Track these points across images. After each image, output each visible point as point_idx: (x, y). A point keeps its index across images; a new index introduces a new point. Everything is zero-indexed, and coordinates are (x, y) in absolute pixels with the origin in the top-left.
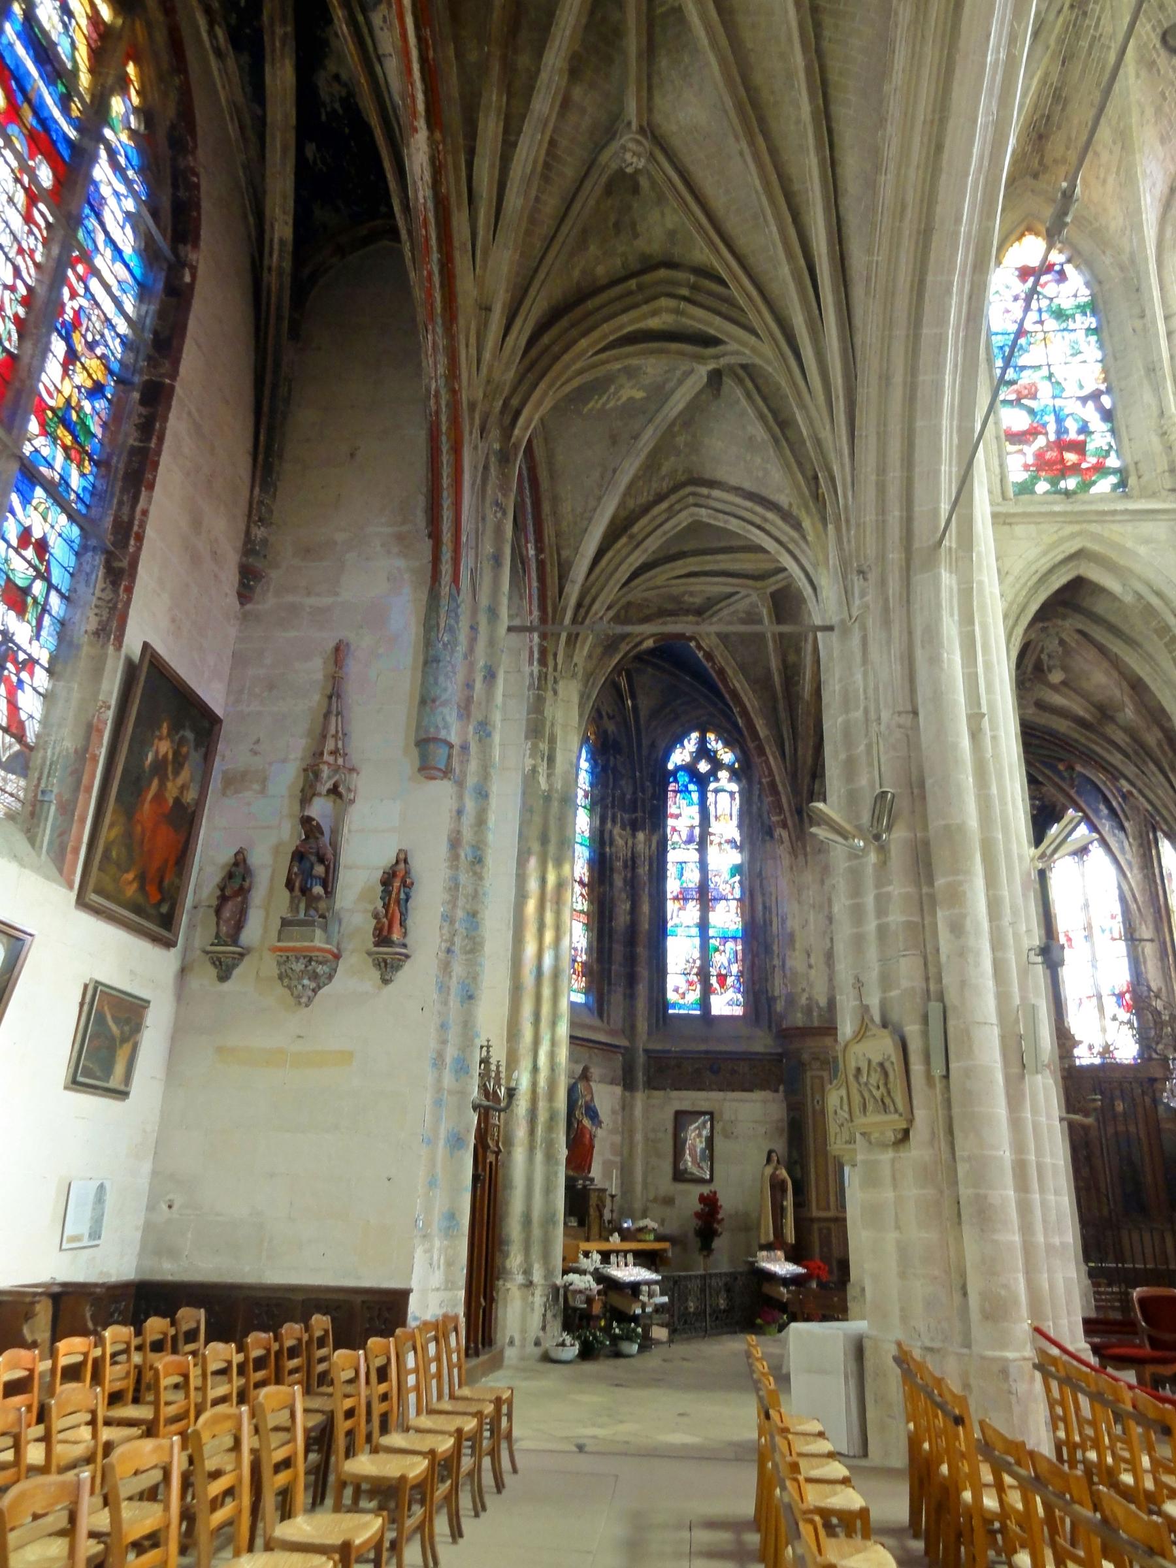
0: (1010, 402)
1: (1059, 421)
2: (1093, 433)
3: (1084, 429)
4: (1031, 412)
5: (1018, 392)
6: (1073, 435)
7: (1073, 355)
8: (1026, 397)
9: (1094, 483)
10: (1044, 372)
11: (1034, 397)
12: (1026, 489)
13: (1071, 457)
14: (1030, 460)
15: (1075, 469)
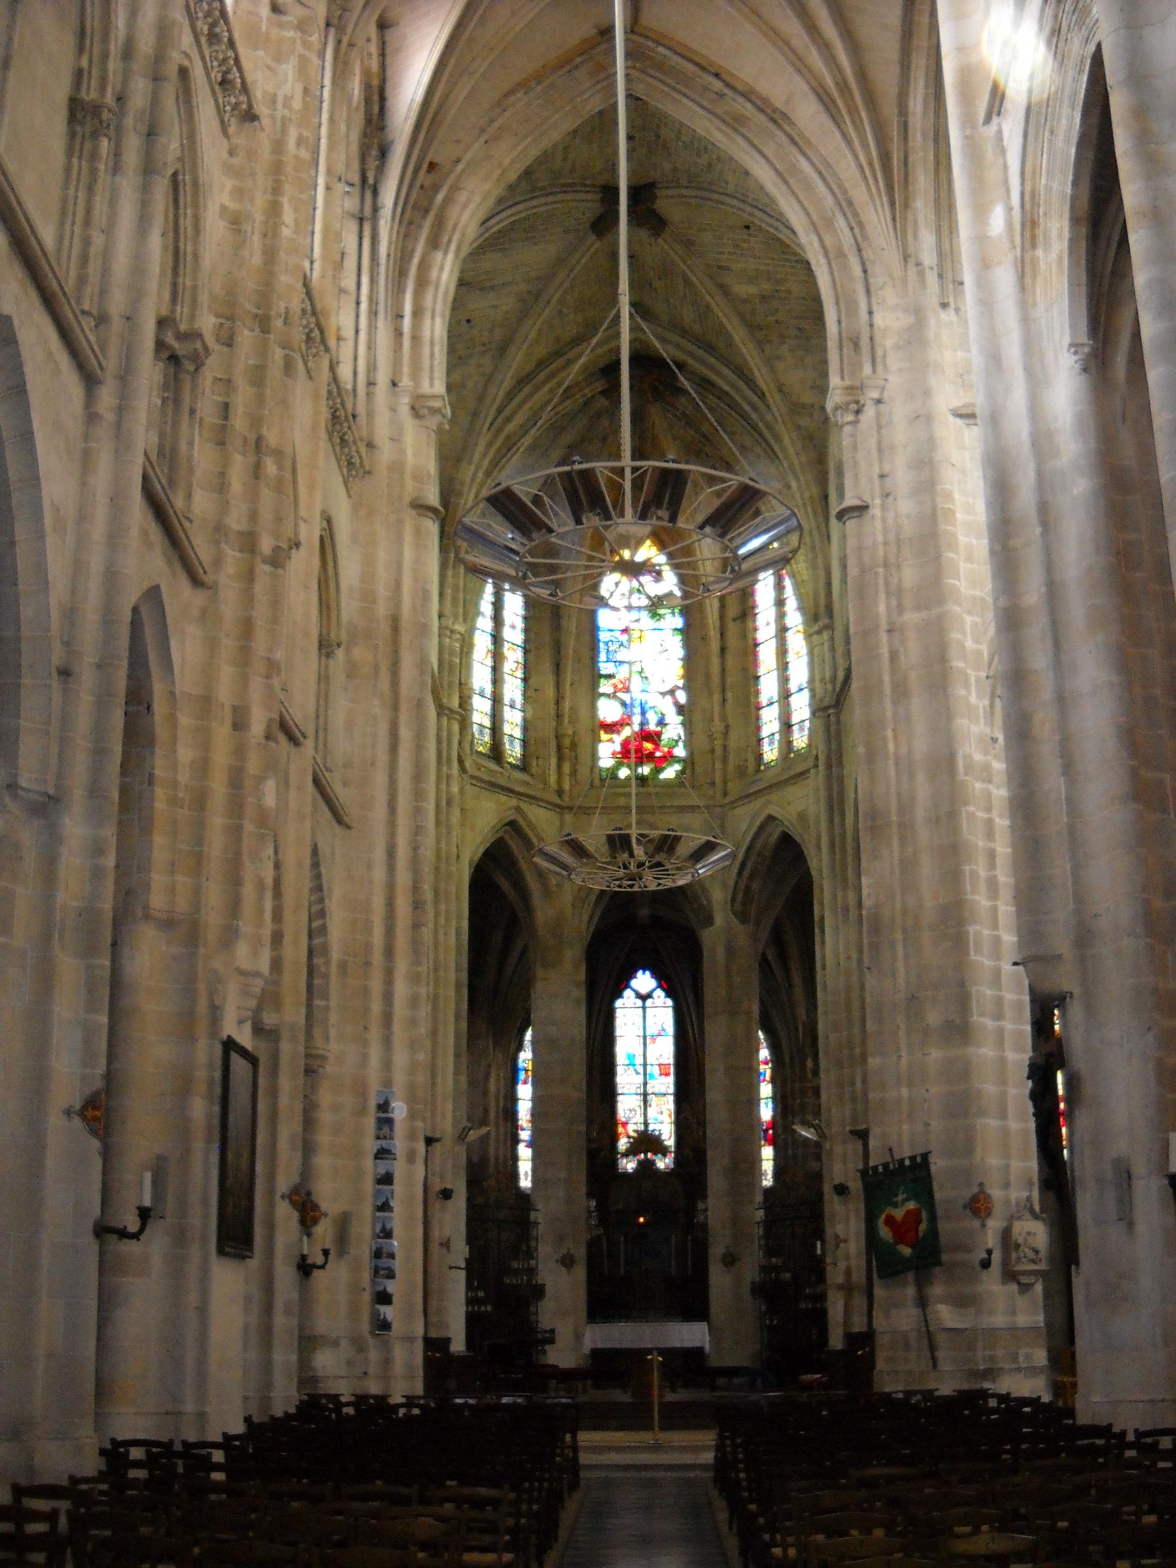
0: (608, 696)
1: (643, 713)
2: (666, 724)
3: (661, 723)
4: (624, 704)
5: (615, 686)
6: (652, 727)
7: (661, 652)
8: (620, 690)
9: (662, 770)
10: (636, 668)
11: (627, 690)
12: (613, 773)
13: (649, 746)
14: (618, 748)
15: (650, 757)
